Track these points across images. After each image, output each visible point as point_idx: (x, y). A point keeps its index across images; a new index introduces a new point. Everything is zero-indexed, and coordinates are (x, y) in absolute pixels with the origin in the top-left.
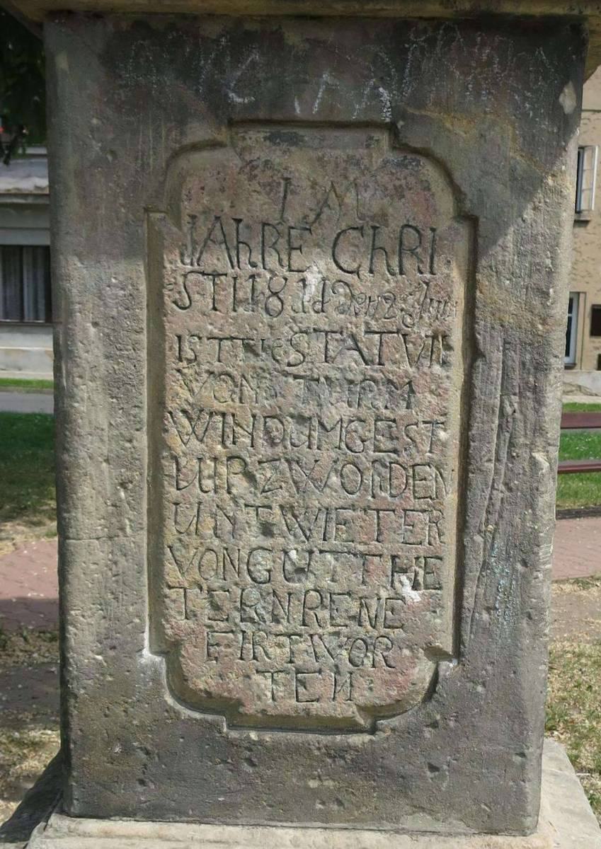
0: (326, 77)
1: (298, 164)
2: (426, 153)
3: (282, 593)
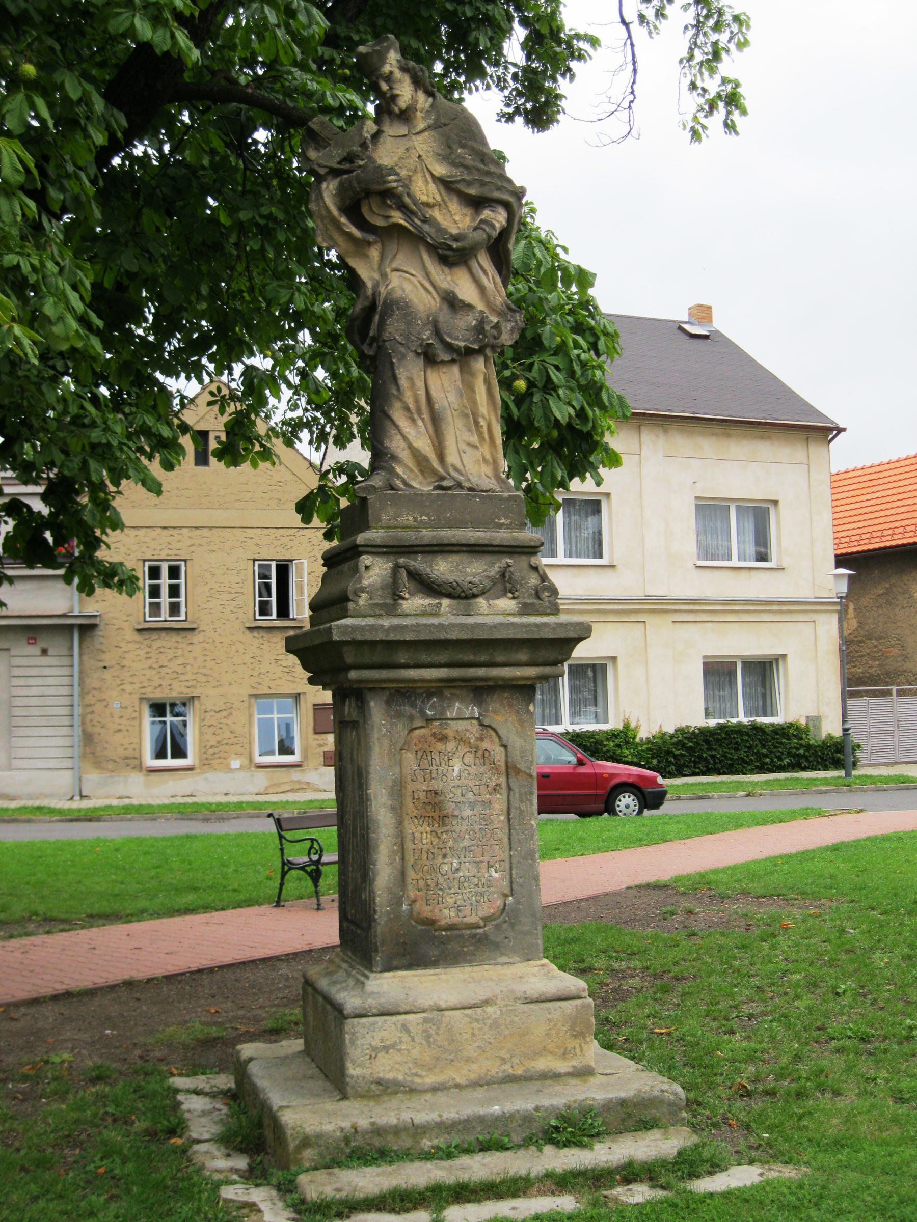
2: (489, 726)
3: (451, 878)
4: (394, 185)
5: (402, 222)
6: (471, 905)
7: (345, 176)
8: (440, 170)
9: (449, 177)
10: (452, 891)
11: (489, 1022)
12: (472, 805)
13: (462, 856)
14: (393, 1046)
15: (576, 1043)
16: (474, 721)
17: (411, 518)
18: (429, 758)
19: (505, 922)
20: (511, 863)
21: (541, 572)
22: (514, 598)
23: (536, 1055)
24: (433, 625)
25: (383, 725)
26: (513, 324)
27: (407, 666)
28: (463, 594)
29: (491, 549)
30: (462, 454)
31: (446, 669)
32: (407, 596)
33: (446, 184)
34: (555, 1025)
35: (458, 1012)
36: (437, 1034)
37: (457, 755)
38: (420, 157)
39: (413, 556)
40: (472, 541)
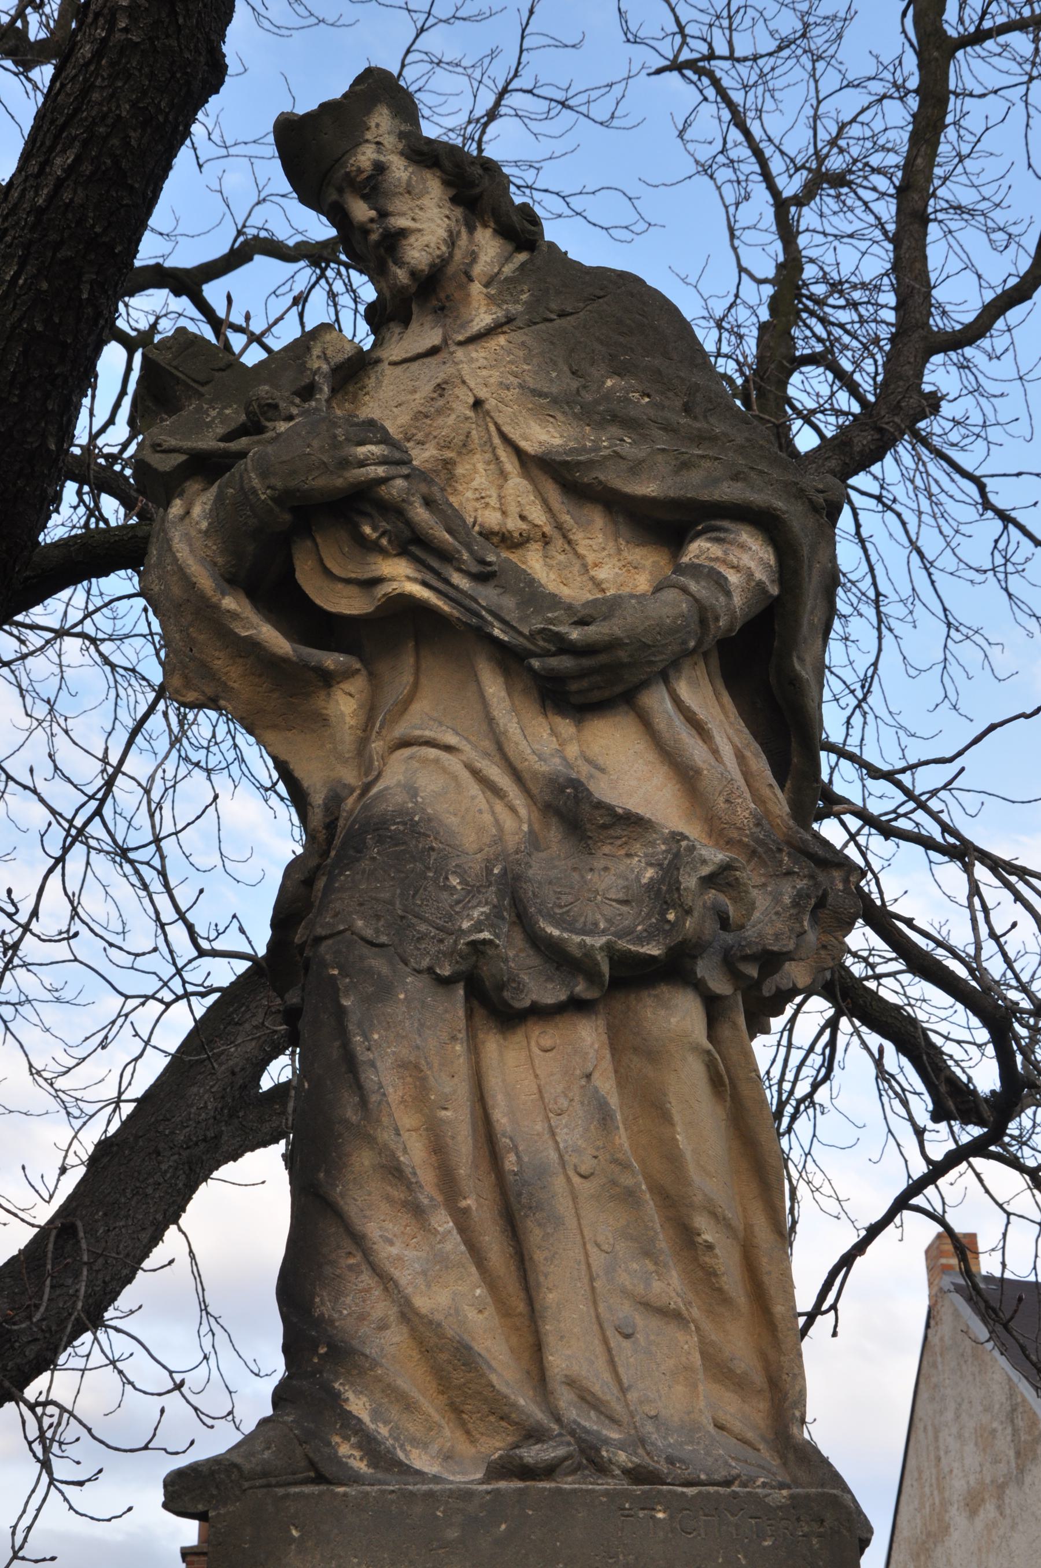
9: (572, 451)
26: (801, 884)
30: (615, 1340)
38: (478, 404)
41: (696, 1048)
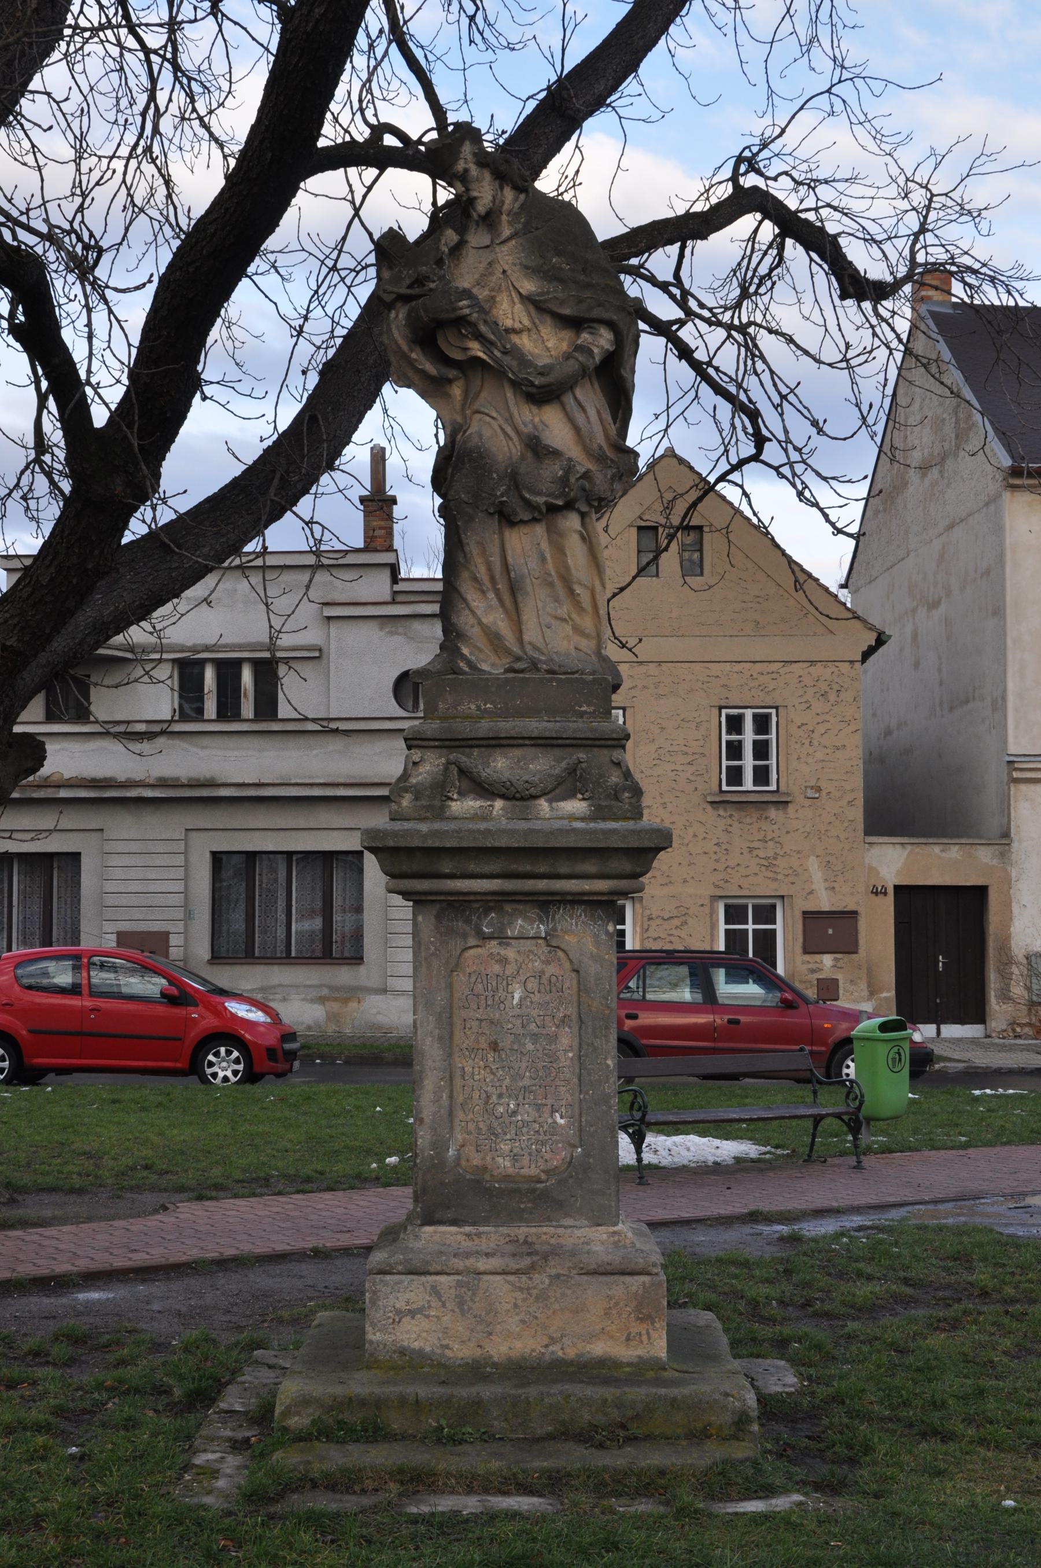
0: (520, 921)
1: (510, 953)
2: (558, 947)
3: (507, 1121)
4: (467, 311)
5: (481, 354)
6: (530, 1154)
7: (414, 303)
8: (528, 286)
9: (538, 295)
10: (508, 1137)
11: (535, 1292)
12: (535, 1037)
13: (521, 1097)
14: (420, 1311)
15: (642, 1328)
16: (540, 941)
17: (473, 707)
18: (485, 982)
19: (571, 1177)
20: (580, 1108)
21: (624, 769)
22: (584, 799)
23: (592, 1337)
24: (479, 831)
25: (432, 943)
26: (614, 471)
27: (452, 876)
28: (518, 795)
29: (560, 742)
30: (545, 629)
31: (499, 881)
32: (455, 796)
33: (535, 304)
34: (617, 1304)
35: (498, 1278)
36: (472, 1300)
37: (518, 979)
38: (504, 272)
39: (467, 750)
40: (535, 734)
41: (576, 531)
